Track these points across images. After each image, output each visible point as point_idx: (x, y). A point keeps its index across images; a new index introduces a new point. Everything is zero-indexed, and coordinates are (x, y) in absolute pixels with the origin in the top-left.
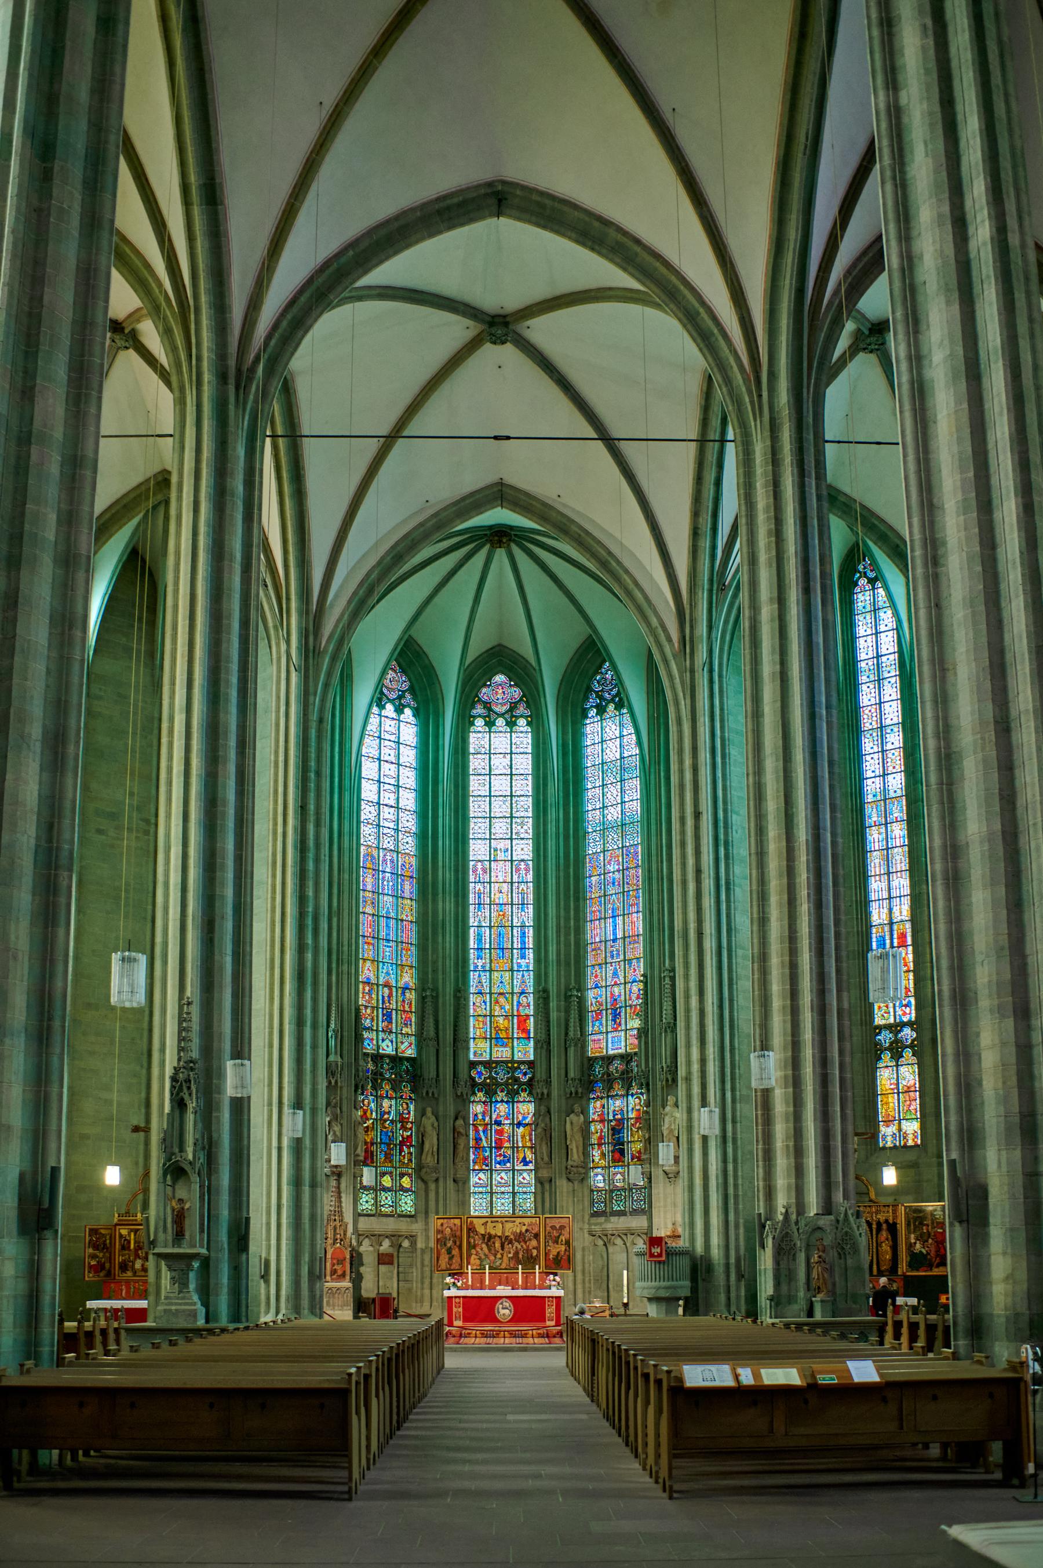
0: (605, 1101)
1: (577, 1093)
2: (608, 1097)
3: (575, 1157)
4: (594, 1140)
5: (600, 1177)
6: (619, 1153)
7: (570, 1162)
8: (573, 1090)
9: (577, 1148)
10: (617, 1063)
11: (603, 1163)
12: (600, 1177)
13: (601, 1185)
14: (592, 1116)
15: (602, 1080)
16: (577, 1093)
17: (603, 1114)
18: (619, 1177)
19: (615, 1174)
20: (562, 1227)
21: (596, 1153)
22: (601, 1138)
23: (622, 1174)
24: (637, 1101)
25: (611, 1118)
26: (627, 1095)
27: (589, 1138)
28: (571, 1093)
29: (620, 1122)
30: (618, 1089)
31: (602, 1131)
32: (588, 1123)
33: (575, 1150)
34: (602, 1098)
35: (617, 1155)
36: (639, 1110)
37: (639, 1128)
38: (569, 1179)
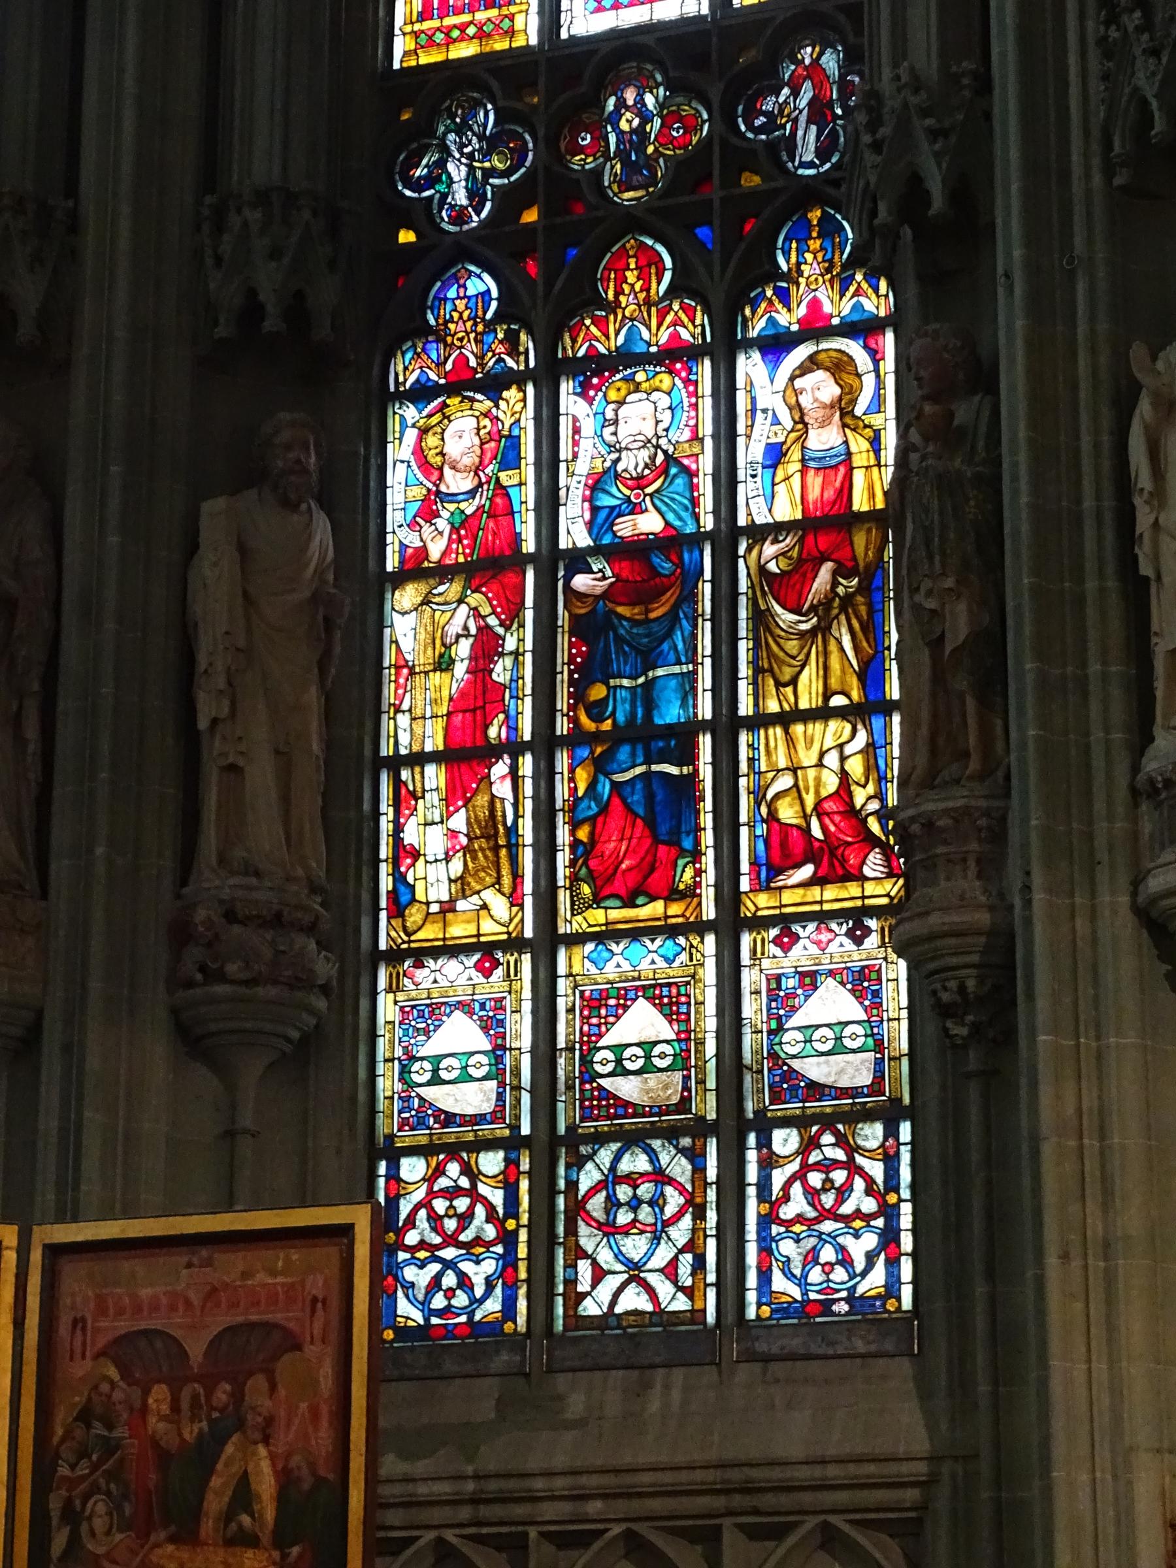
0: (518, 407)
1: (297, 311)
2: (546, 379)
3: (264, 834)
4: (416, 720)
5: (460, 1035)
6: (643, 824)
7: (213, 884)
8: (269, 282)
9: (283, 757)
10: (637, 107)
11: (496, 913)
12: (460, 1035)
13: (473, 1098)
14: (400, 535)
15: (495, 247)
16: (297, 311)
17: (501, 507)
18: (641, 1022)
19: (603, 1005)
20: (255, 1348)
21: (429, 835)
22: (481, 698)
23: (671, 1000)
24: (821, 388)
25: (574, 532)
26: (725, 348)
27: (372, 710)
28: (252, 311)
29: (657, 571)
30: (642, 305)
31: (487, 647)
32: (362, 584)
33: (261, 775)
34: (494, 385)
35: (621, 847)
36: (841, 466)
37: (825, 613)
38: (194, 1041)
